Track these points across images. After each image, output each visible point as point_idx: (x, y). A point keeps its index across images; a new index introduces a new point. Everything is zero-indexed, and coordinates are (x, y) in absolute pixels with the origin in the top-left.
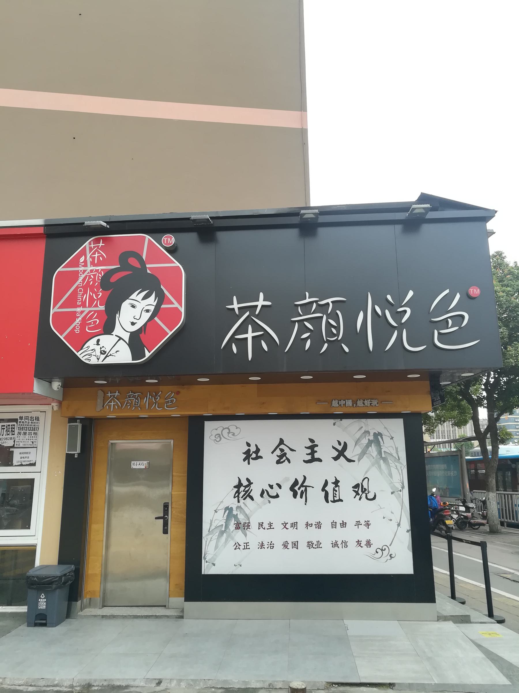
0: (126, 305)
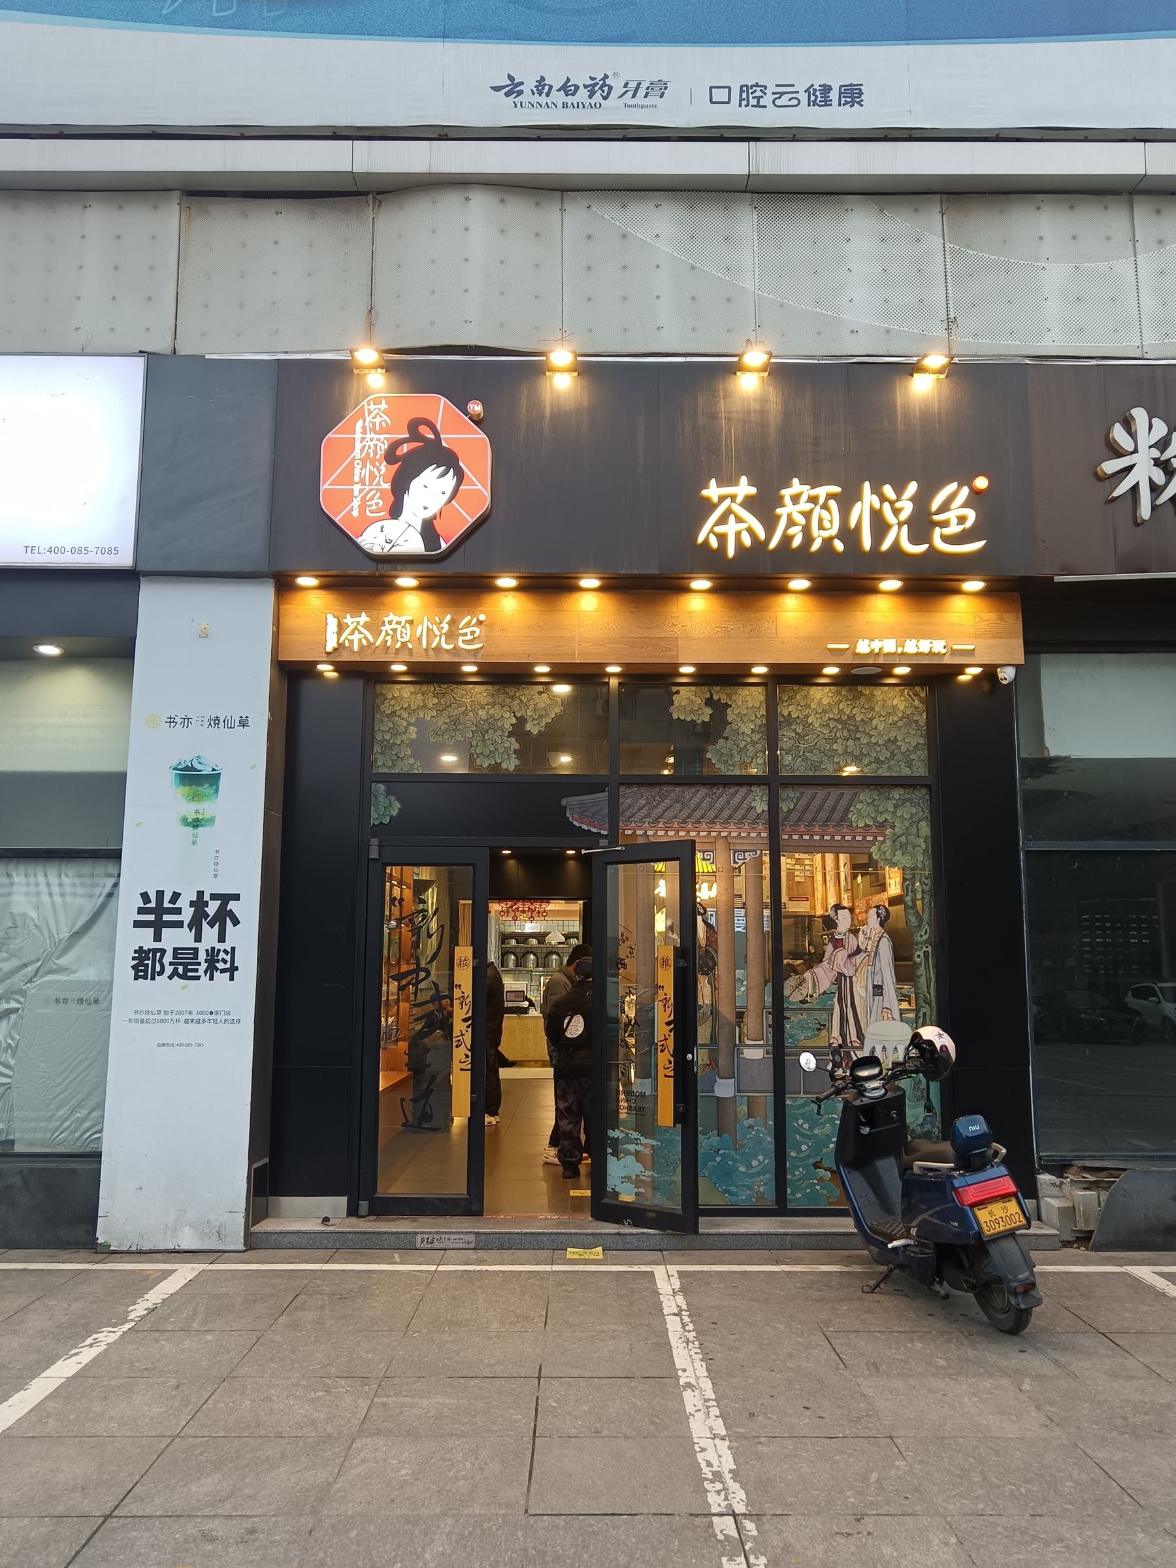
0: (416, 484)
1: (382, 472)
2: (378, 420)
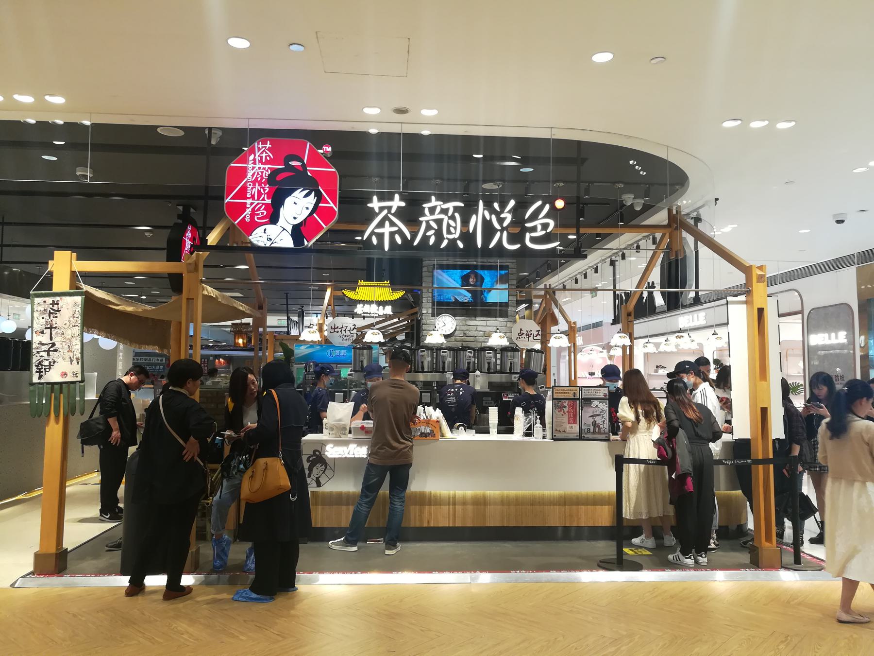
0: (289, 201)
1: (266, 192)
2: (264, 155)
